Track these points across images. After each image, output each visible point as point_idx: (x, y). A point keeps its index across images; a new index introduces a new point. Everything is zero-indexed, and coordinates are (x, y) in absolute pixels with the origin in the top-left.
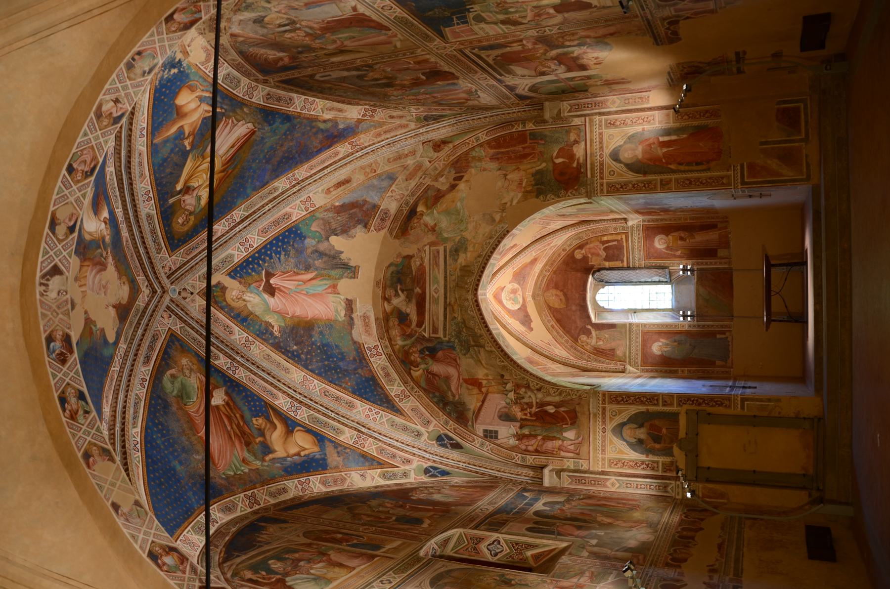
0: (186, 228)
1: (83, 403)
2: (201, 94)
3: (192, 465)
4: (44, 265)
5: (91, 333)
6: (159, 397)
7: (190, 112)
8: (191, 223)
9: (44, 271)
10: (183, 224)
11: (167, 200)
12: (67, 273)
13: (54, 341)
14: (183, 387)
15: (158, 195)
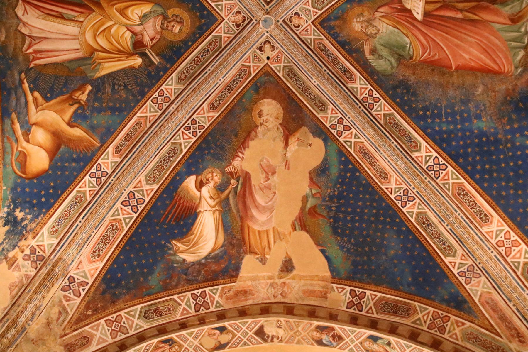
0: (185, 15)
1: (379, 342)
2: (21, 139)
3: (488, 105)
4: (256, 343)
5: (313, 212)
6: (394, 88)
7: (49, 131)
8: (176, 11)
9: (261, 341)
10: (181, 22)
11: (157, 68)
12: (262, 322)
13: (321, 339)
14: (386, 45)
15: (154, 85)
